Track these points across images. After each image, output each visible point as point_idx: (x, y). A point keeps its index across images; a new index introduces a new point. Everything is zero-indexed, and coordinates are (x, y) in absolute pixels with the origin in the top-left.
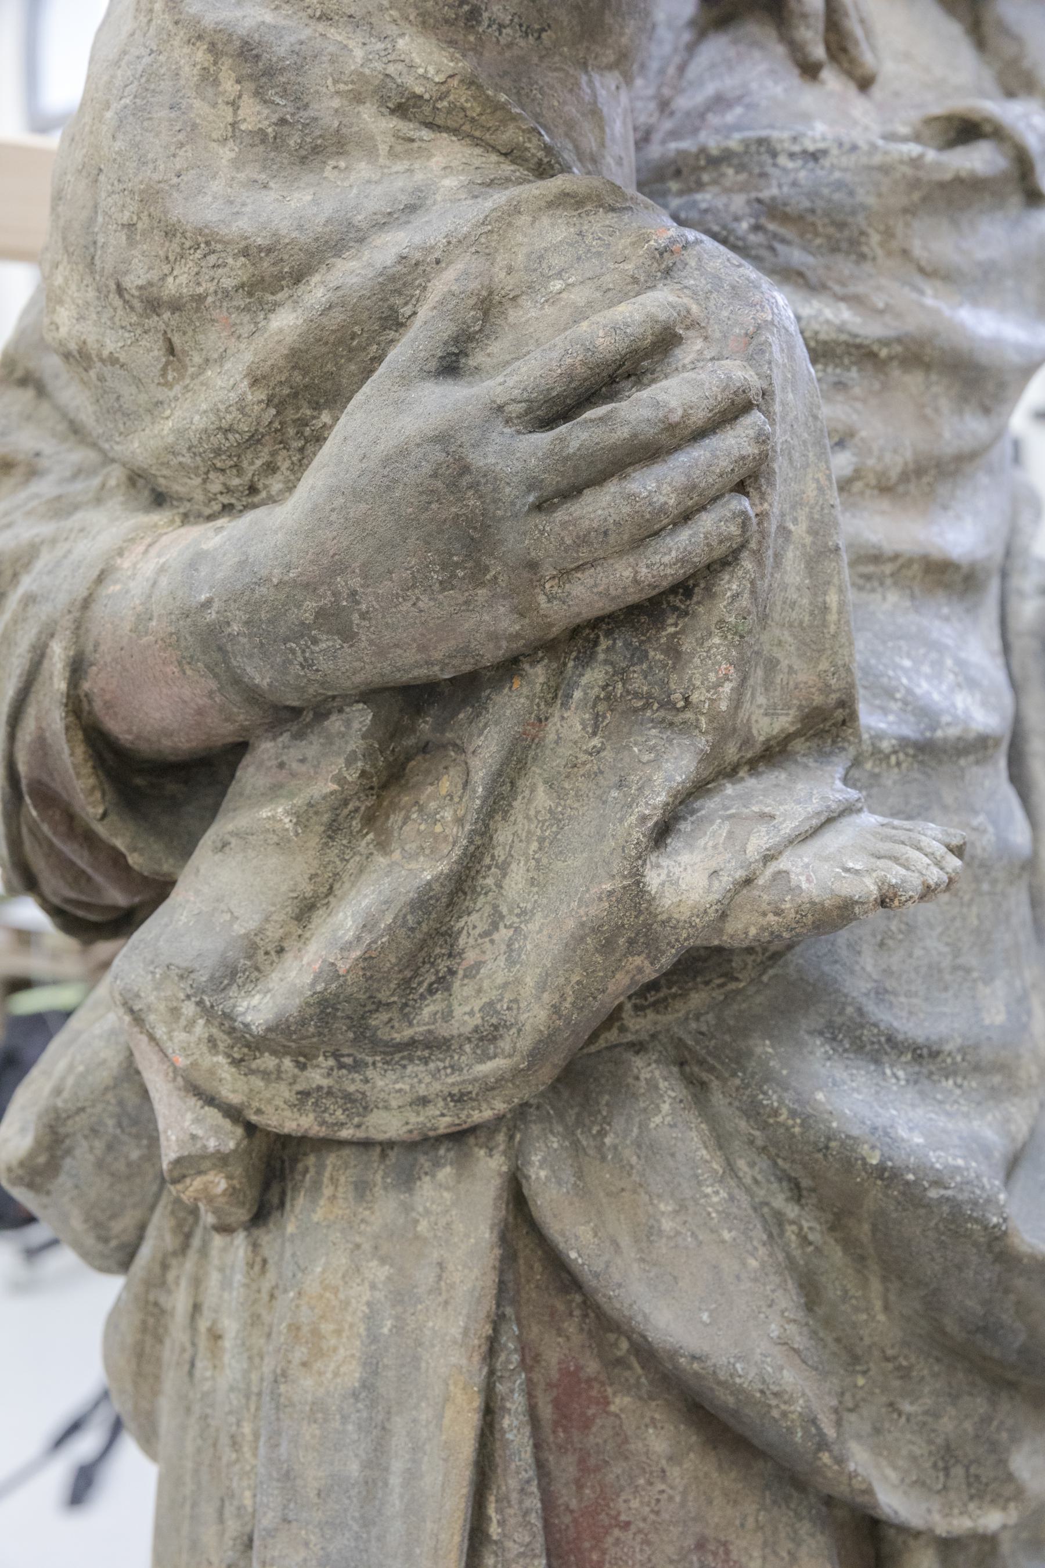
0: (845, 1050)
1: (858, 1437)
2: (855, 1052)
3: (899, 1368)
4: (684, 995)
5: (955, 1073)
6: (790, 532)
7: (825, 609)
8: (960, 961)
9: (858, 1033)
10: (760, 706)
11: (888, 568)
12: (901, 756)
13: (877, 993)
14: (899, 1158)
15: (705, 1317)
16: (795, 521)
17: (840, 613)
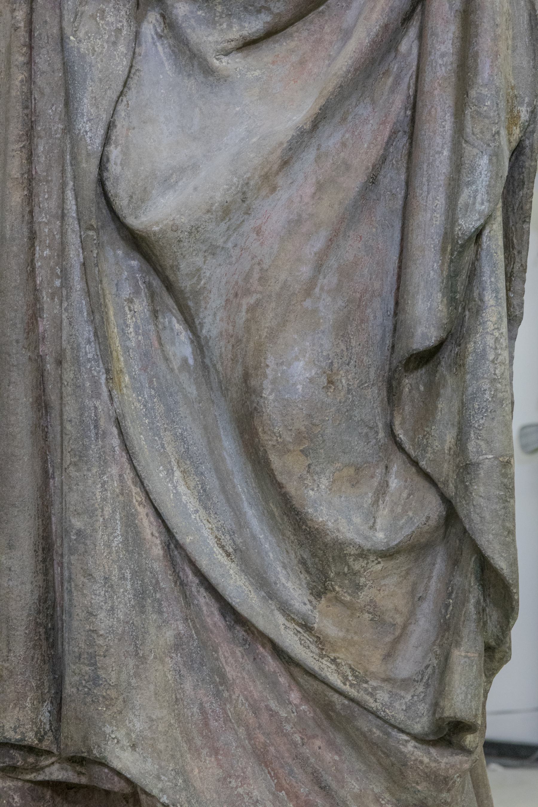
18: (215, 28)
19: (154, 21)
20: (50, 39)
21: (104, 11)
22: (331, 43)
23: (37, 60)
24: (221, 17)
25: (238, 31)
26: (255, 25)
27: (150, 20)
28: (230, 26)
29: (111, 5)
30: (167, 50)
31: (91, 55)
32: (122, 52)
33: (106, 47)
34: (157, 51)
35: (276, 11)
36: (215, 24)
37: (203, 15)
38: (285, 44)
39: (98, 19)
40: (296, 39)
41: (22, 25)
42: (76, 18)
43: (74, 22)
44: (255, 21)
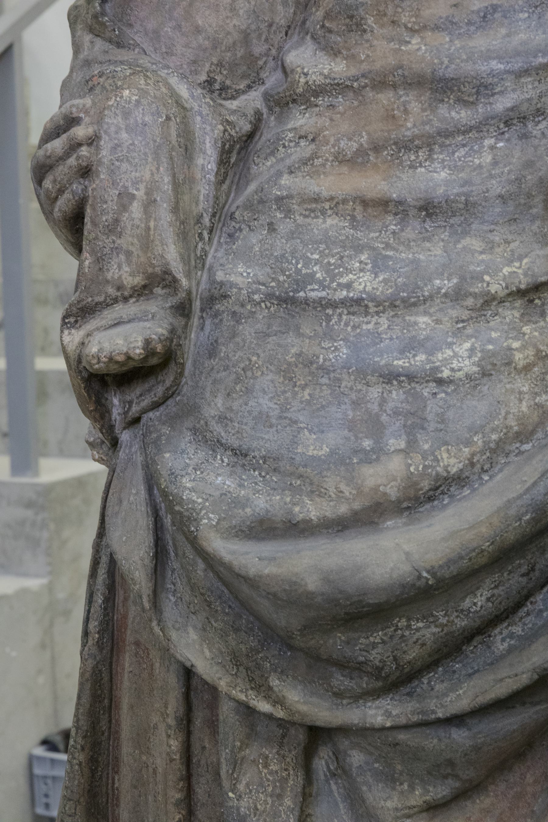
0: (199, 441)
1: (195, 627)
2: (203, 443)
3: (206, 600)
4: (144, 400)
5: (260, 469)
6: (134, 195)
7: (149, 228)
8: (285, 415)
9: (205, 434)
10: (127, 272)
11: (327, 207)
12: (269, 305)
13: (220, 417)
14: (173, 489)
15: (124, 538)
16: (137, 189)
17: (155, 230)
18: (394, 789)
19: (326, 757)
20: (210, 768)
21: (267, 757)
22: (534, 795)
23: (198, 790)
24: (401, 774)
25: (421, 795)
26: (440, 791)
27: (322, 755)
28: (412, 788)
29: (274, 751)
30: (341, 790)
31: (252, 816)
32: (289, 806)
33: (270, 803)
34: (331, 791)
35: (465, 777)
36: (395, 783)
37: (381, 768)
38: (478, 801)
39: (260, 766)
40: (492, 794)
41: (177, 757)
42: (235, 768)
43: (232, 774)
44: (441, 785)
